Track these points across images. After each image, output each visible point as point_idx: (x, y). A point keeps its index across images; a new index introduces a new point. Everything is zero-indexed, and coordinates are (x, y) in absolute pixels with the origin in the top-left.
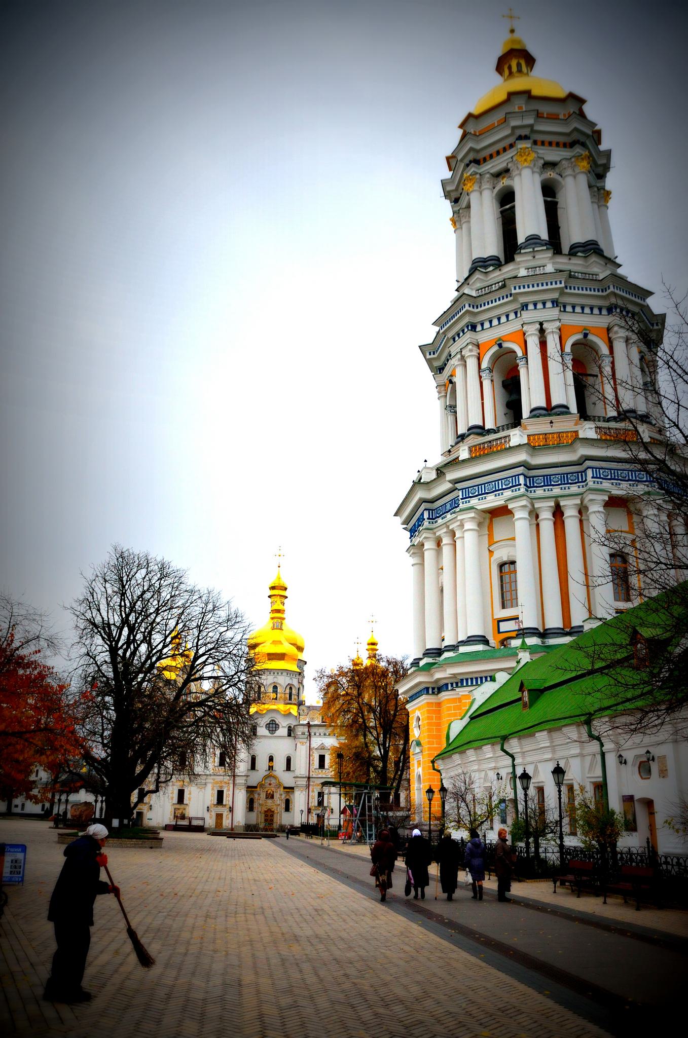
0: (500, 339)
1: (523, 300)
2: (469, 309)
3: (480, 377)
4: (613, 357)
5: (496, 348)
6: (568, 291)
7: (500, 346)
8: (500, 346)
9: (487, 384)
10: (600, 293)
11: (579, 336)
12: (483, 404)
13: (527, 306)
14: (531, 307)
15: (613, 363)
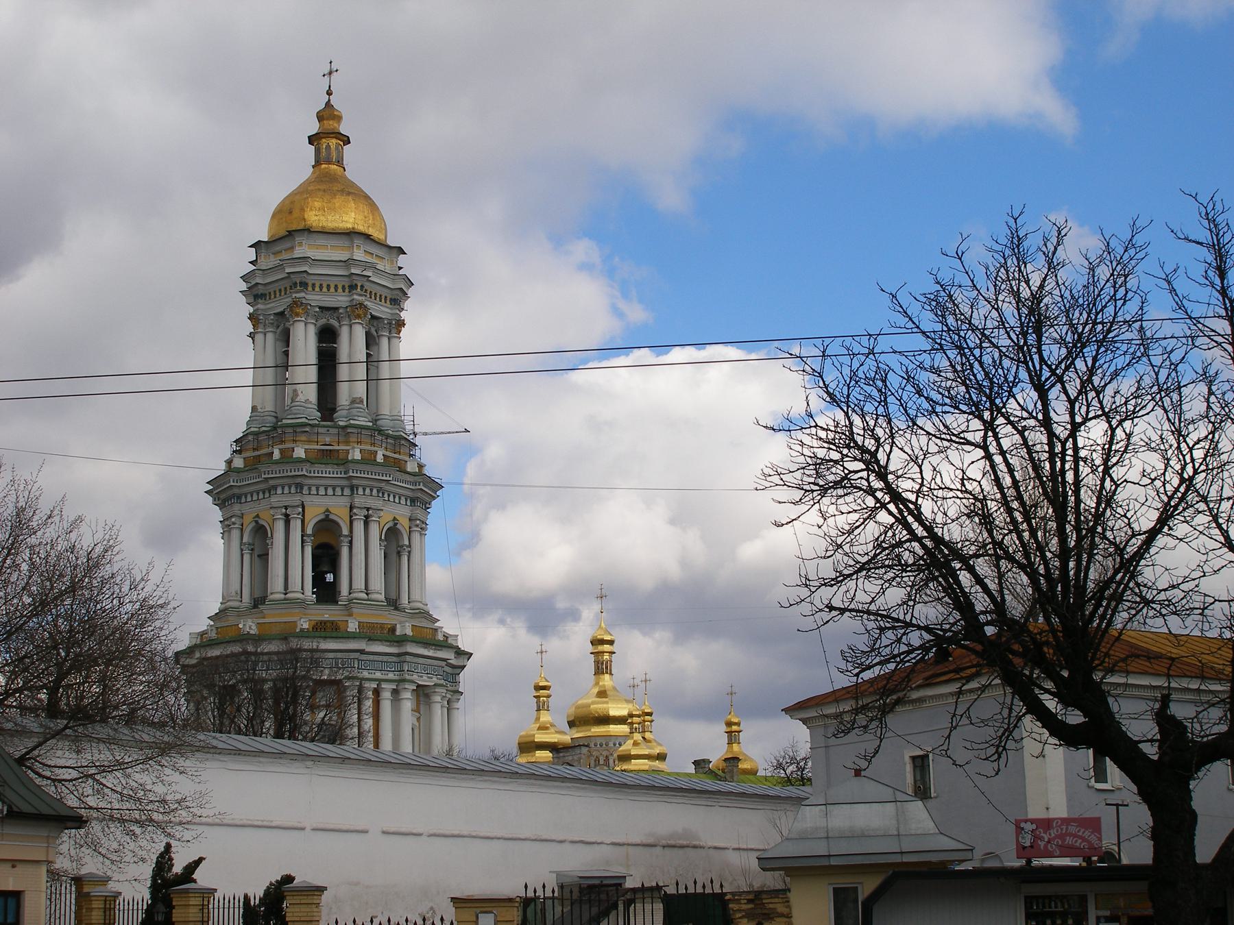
0: (257, 516)
1: (272, 482)
2: (232, 484)
3: (242, 550)
4: (352, 537)
5: (254, 524)
6: (312, 474)
7: (257, 522)
8: (257, 522)
9: (247, 558)
10: (343, 475)
11: (322, 517)
12: (242, 575)
13: (275, 488)
14: (279, 491)
15: (351, 542)
